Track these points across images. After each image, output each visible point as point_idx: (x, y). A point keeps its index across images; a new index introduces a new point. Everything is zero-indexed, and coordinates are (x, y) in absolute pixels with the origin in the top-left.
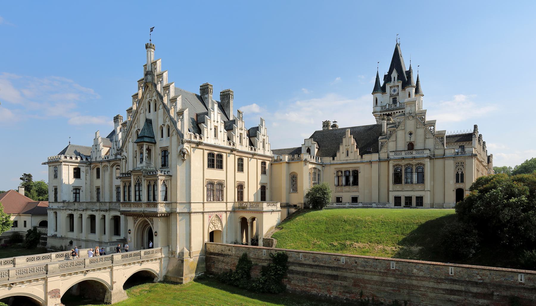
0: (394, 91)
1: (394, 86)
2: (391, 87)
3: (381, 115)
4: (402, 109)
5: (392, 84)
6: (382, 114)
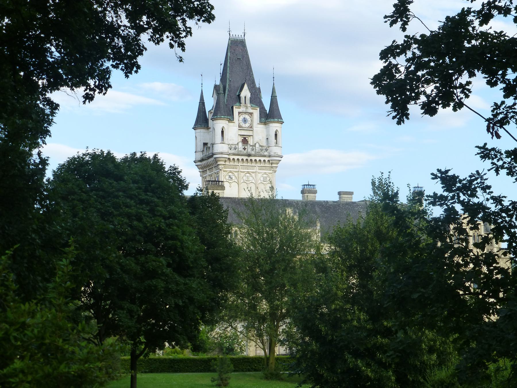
0: (245, 121)
1: (245, 113)
2: (239, 113)
3: (229, 159)
4: (265, 156)
5: (242, 109)
6: (232, 157)
